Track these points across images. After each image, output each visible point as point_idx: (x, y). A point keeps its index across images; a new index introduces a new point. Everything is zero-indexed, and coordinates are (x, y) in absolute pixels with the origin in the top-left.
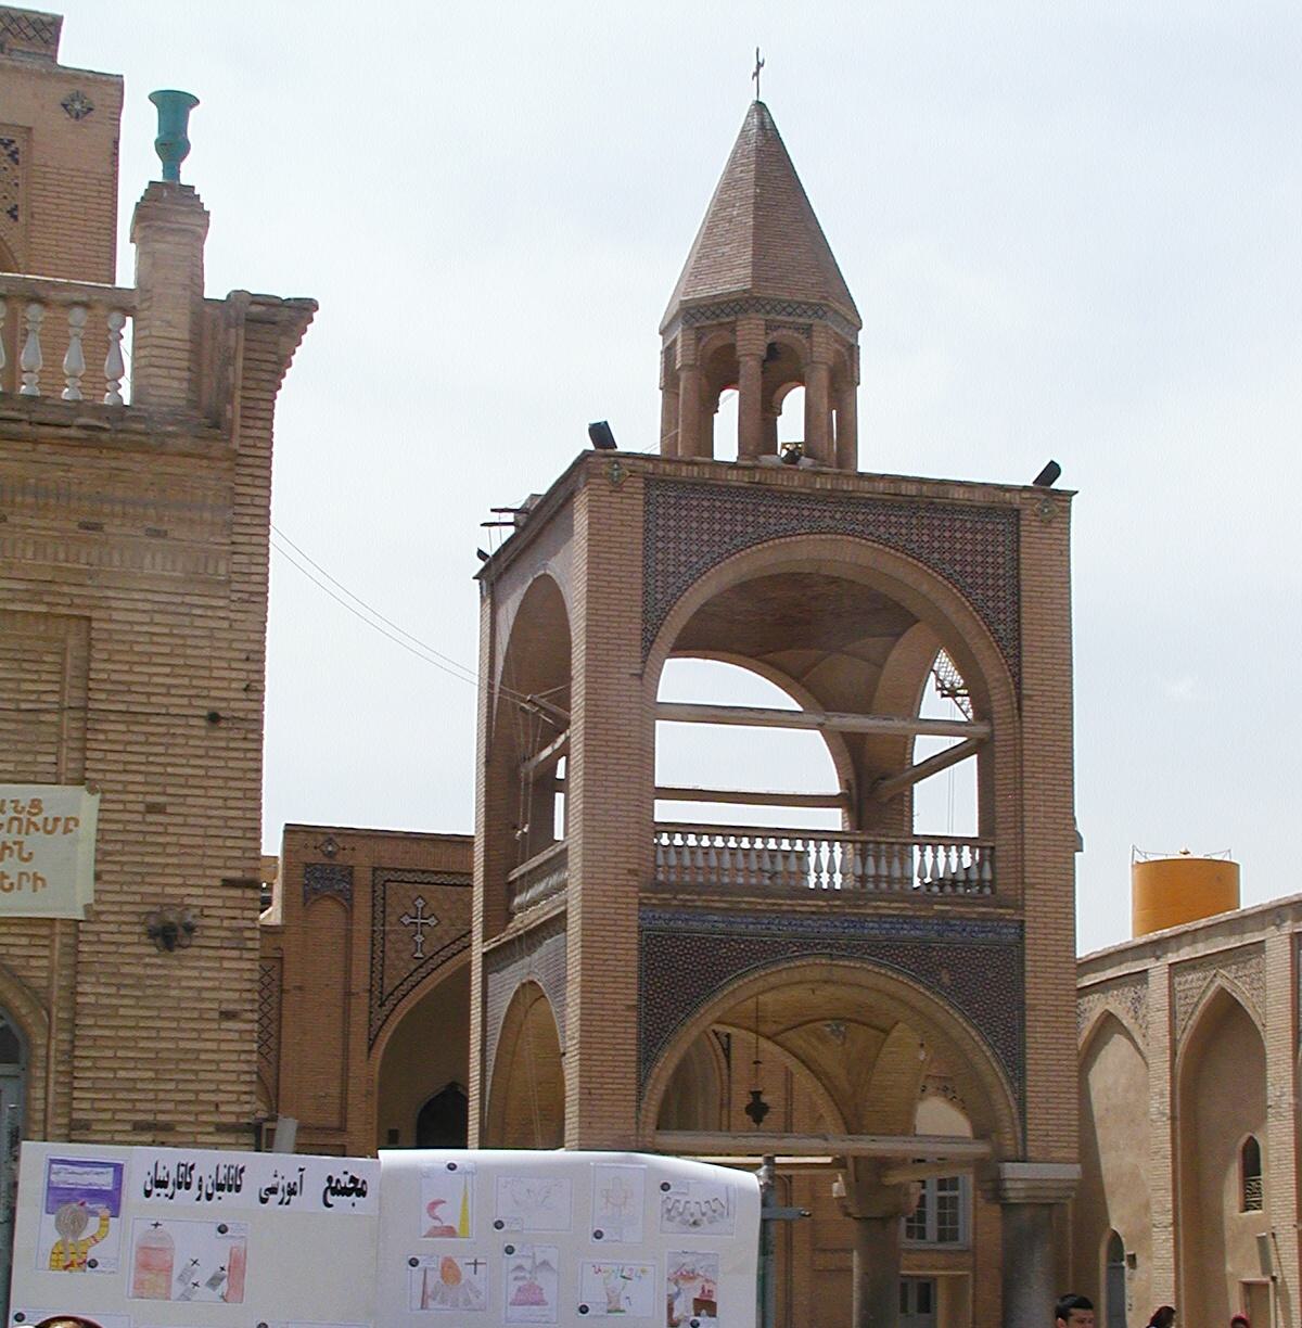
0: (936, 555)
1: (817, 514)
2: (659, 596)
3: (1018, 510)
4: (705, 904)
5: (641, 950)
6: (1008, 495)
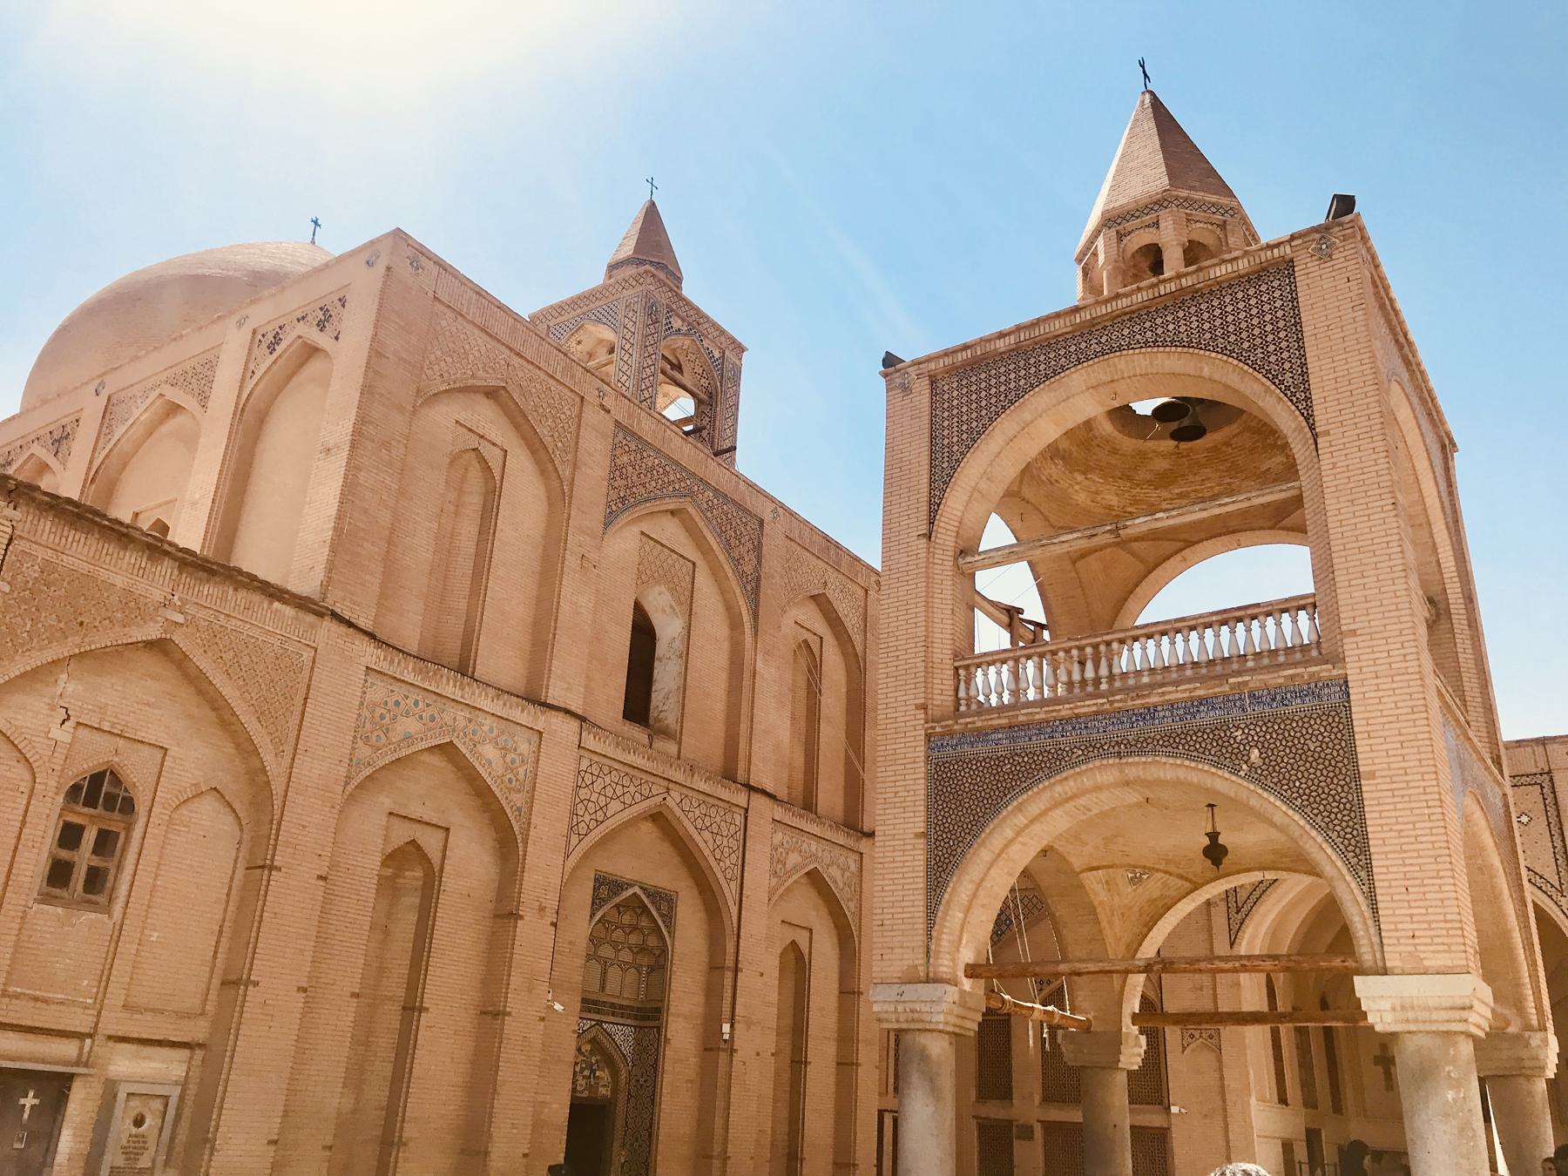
0: (1208, 336)
1: (1083, 345)
5: (930, 777)
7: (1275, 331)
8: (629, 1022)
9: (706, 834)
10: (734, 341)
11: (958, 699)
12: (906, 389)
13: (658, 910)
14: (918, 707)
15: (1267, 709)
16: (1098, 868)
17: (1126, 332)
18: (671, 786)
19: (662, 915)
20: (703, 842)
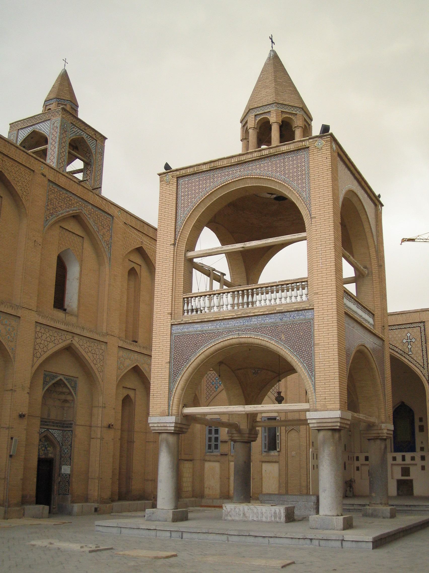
1: (235, 171)
2: (182, 216)
3: (308, 147)
4: (193, 321)
6: (303, 143)
7: (302, 175)
8: (60, 428)
9: (90, 354)
10: (101, 135)
11: (184, 311)
12: (168, 183)
13: (71, 384)
14: (168, 313)
15: (288, 319)
16: (241, 369)
17: (250, 168)
18: (74, 335)
19: (72, 387)
20: (88, 357)
